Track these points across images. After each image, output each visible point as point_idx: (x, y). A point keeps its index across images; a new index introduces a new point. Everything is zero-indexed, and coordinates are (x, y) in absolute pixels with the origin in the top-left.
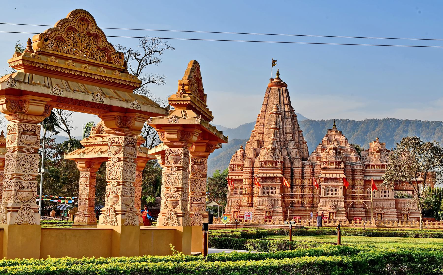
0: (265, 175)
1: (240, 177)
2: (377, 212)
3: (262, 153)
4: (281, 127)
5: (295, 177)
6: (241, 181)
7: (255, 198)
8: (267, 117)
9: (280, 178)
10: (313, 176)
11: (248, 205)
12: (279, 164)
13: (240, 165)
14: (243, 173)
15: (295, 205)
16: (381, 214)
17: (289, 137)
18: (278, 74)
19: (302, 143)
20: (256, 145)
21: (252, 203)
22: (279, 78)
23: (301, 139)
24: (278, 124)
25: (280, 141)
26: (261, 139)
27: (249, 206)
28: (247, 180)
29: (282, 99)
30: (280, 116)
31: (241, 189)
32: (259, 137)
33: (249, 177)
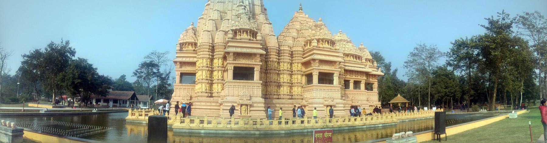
1: (191, 60)
5: (271, 59)
6: (193, 64)
7: (215, 86)
9: (261, 55)
10: (292, 60)
11: (207, 95)
21: (211, 93)
27: (207, 97)
28: (204, 60)
31: (194, 74)
33: (208, 56)
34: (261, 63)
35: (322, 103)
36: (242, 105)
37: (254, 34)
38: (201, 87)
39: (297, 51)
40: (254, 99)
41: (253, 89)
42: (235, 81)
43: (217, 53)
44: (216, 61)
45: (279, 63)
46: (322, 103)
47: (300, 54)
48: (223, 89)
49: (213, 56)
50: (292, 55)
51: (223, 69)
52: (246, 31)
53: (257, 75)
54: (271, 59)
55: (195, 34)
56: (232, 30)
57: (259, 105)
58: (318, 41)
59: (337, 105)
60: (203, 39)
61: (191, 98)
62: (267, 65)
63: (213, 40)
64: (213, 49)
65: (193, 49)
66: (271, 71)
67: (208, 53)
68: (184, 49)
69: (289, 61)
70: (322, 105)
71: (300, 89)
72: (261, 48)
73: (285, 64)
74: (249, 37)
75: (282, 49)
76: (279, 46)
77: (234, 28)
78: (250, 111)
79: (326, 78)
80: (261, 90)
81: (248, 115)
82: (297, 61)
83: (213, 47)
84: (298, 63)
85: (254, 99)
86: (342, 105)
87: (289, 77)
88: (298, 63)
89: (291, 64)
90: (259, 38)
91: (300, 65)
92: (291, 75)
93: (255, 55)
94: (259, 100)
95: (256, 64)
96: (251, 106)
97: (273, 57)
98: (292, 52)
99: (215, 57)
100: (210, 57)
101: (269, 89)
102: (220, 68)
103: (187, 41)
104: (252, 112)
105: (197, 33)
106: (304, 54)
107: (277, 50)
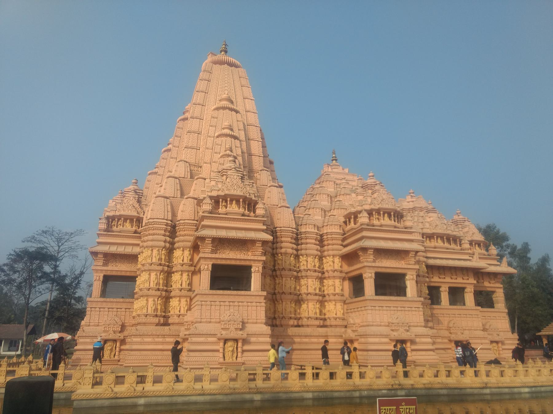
1: (129, 250)
5: (283, 250)
6: (133, 258)
7: (174, 303)
9: (264, 243)
11: (156, 320)
20: (181, 170)
21: (166, 317)
24: (235, 128)
26: (192, 161)
27: (157, 325)
28: (155, 252)
31: (132, 279)
32: (189, 156)
33: (163, 244)
34: (264, 258)
35: (386, 336)
36: (226, 341)
37: (250, 204)
38: (144, 306)
39: (332, 233)
40: (251, 328)
41: (249, 307)
42: (214, 292)
43: (182, 238)
44: (177, 253)
45: (297, 257)
46: (386, 336)
47: (336, 239)
48: (189, 309)
49: (172, 244)
50: (321, 241)
51: (192, 268)
52: (236, 199)
53: (256, 280)
54: (283, 250)
55: (139, 201)
56: (211, 198)
57: (261, 339)
58: (370, 213)
59: (418, 340)
60: (155, 211)
61: (123, 327)
62: (275, 261)
63: (174, 214)
64: (172, 230)
65: (134, 228)
66: (283, 273)
67: (163, 238)
68: (114, 228)
69: (316, 252)
70: (386, 340)
71: (339, 306)
72: (263, 230)
73: (310, 259)
74: (241, 210)
75: (303, 230)
76: (296, 224)
77: (214, 194)
78: (243, 351)
79: (390, 284)
80: (264, 309)
81: (239, 360)
82: (331, 253)
83: (174, 227)
84: (334, 256)
86: (429, 340)
87: (317, 284)
88: (334, 256)
89: (321, 258)
90: (260, 211)
91: (337, 260)
92: (321, 280)
93: (253, 242)
94: (259, 328)
95: (255, 259)
96: (245, 341)
97: (287, 246)
98: (321, 236)
99: (176, 245)
100: (168, 245)
101: (280, 307)
102: (185, 268)
103: (122, 213)
104: (246, 354)
105: (143, 199)
106: (344, 240)
107: (293, 232)
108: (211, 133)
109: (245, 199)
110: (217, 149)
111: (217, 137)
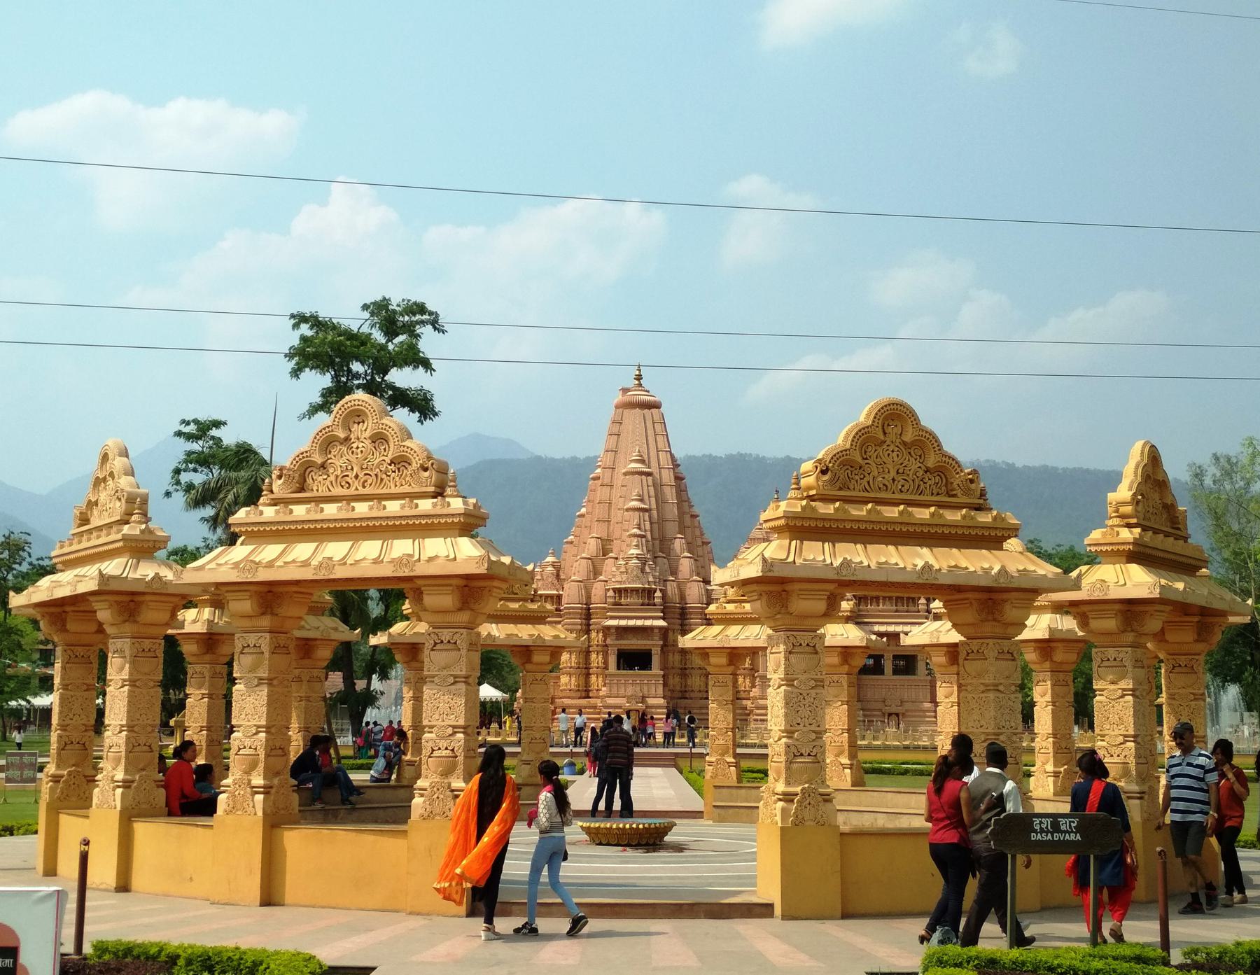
0: (623, 623)
2: (889, 710)
3: (609, 567)
4: (654, 506)
7: (593, 678)
8: (619, 479)
9: (660, 628)
12: (658, 594)
13: (551, 597)
14: (560, 616)
15: (692, 695)
16: (897, 715)
17: (671, 528)
18: (639, 378)
19: (699, 543)
21: (588, 691)
22: (640, 385)
23: (698, 533)
24: (646, 497)
25: (653, 539)
29: (651, 438)
30: (650, 478)
37: (650, 593)
49: (589, 625)
52: (635, 591)
53: (656, 661)
56: (614, 590)
63: (589, 597)
64: (587, 614)
85: (651, 701)
93: (651, 628)
95: (655, 645)
108: (620, 505)
109: (644, 590)
110: (626, 526)
111: (627, 510)
